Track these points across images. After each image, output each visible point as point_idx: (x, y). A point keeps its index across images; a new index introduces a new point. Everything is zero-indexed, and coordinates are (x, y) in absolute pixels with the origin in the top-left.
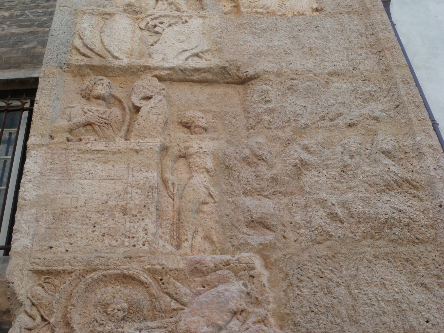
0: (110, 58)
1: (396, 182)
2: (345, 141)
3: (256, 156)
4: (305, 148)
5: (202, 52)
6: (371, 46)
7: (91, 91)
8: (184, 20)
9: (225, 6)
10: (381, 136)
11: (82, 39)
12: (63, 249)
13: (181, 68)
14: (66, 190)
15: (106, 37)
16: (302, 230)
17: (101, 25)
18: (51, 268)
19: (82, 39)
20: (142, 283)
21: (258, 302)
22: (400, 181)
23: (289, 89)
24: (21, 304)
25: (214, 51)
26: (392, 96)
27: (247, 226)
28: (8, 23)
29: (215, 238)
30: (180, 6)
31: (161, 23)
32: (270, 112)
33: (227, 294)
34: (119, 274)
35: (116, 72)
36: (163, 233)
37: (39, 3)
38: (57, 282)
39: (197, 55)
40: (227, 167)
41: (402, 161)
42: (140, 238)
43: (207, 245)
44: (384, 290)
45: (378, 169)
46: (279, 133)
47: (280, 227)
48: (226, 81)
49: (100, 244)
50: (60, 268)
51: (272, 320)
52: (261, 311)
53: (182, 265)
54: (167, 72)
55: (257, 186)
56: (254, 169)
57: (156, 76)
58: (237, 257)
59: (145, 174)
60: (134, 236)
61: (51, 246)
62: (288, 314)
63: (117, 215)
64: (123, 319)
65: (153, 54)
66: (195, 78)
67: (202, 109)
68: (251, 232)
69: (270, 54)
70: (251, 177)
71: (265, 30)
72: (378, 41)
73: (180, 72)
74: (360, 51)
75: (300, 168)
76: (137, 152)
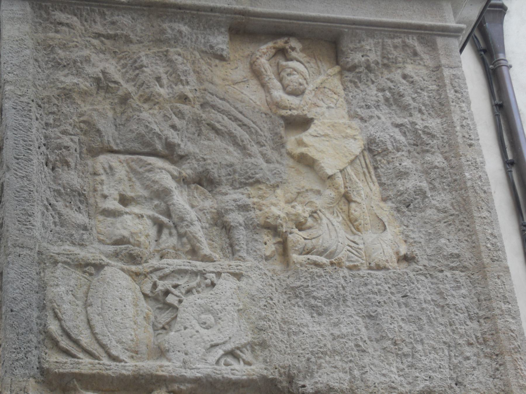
0: (105, 361)
5: (238, 348)
6: (485, 341)
8: (208, 281)
9: (266, 244)
11: (60, 320)
15: (96, 316)
17: (85, 288)
19: (60, 320)
25: (256, 345)
30: (198, 244)
31: (176, 286)
39: (232, 353)
54: (189, 386)
65: (168, 351)
69: (335, 351)
71: (327, 302)
74: (469, 352)
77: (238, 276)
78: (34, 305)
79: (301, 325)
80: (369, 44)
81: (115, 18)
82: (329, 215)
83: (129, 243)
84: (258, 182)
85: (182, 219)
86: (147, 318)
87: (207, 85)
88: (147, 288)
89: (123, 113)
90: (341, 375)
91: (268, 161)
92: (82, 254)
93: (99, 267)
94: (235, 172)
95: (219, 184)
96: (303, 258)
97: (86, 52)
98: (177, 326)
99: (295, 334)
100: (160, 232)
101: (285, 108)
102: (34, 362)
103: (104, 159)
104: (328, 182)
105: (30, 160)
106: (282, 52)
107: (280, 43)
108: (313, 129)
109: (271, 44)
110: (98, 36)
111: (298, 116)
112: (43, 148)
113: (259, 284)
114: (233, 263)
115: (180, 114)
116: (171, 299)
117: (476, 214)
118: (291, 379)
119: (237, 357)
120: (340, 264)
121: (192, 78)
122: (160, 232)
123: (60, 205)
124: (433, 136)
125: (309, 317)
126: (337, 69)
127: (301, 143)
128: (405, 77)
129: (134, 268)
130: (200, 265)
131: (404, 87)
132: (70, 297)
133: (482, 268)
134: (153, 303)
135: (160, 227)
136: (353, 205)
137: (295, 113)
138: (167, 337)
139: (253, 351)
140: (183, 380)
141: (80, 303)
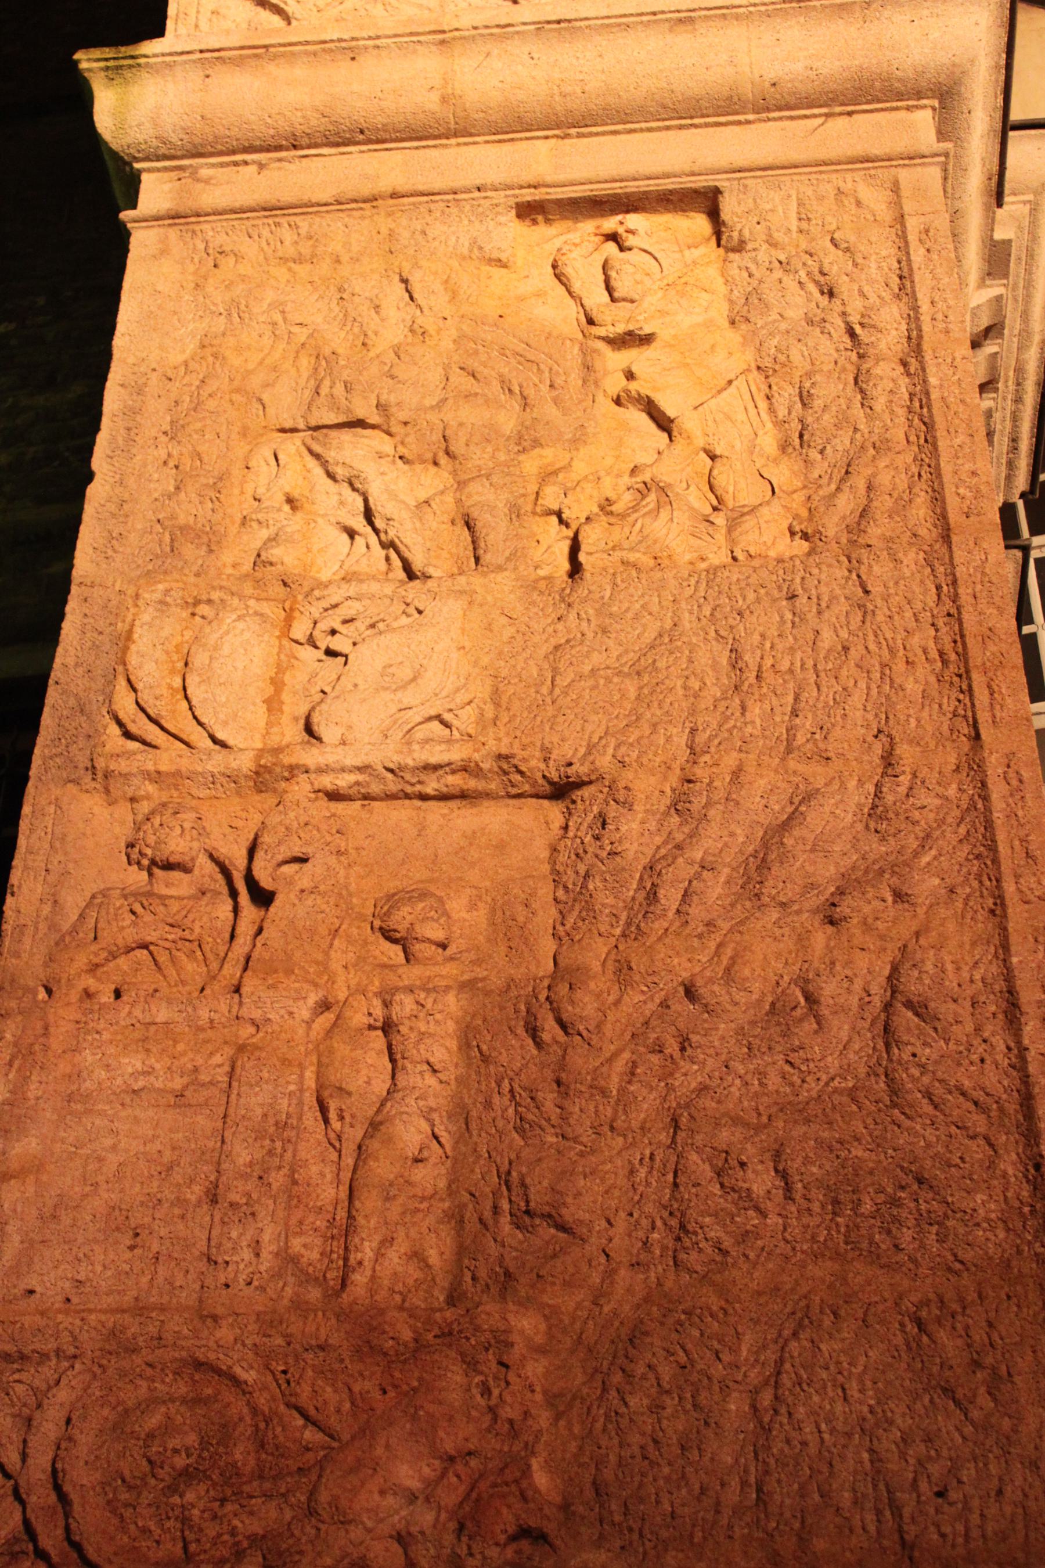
11: (135, 690)
13: (391, 766)
22: (938, 1090)
34: (181, 1360)
35: (218, 786)
36: (305, 1246)
42: (242, 1266)
44: (839, 1407)
48: (514, 791)
54: (352, 778)
60: (227, 1259)
61: (29, 1287)
73: (389, 775)
75: (672, 1057)
107: (610, 224)
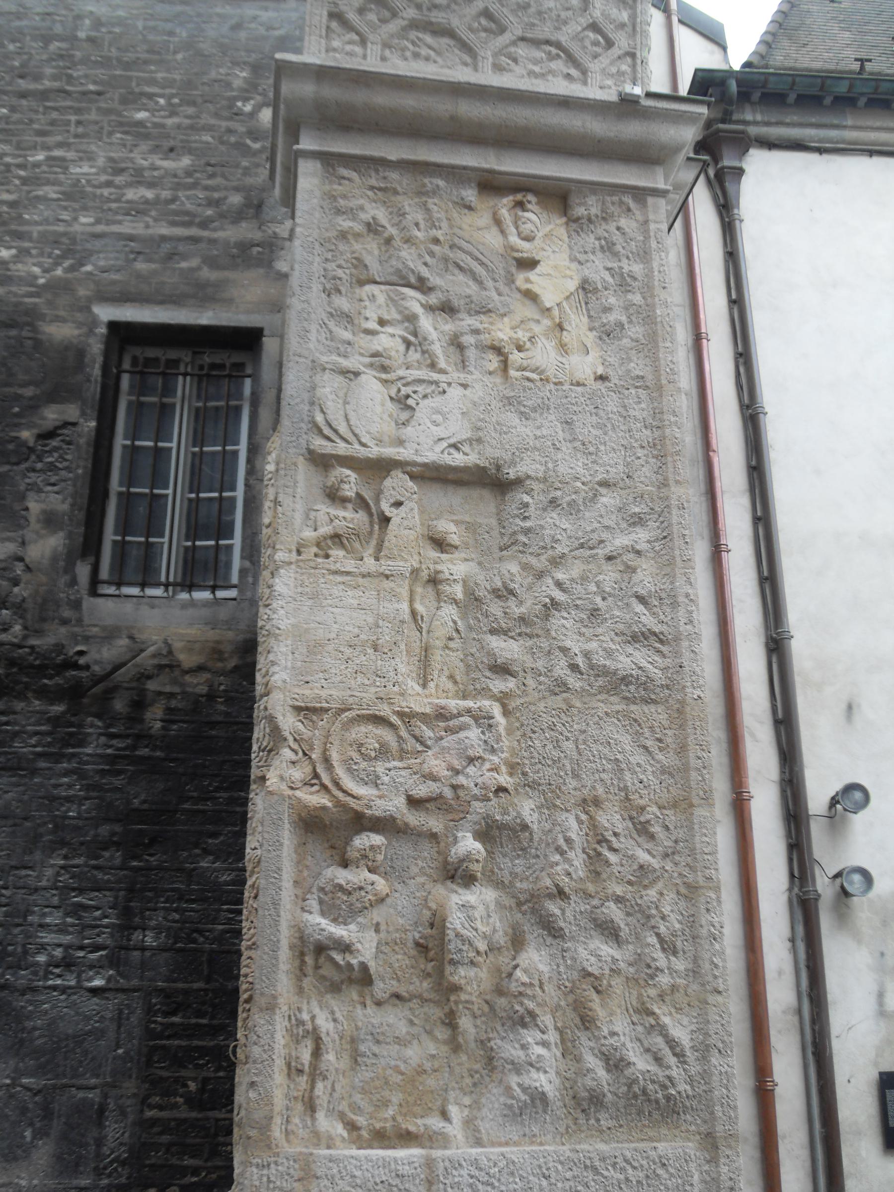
0: (357, 446)
1: (643, 634)
2: (601, 577)
3: (506, 588)
4: (559, 584)
6: (655, 445)
7: (337, 490)
10: (639, 575)
11: (324, 413)
12: (319, 685)
14: (318, 619)
16: (542, 678)
17: (345, 390)
18: (309, 705)
19: (324, 413)
20: (391, 725)
21: (493, 751)
23: (551, 502)
24: (285, 739)
26: (662, 522)
27: (490, 670)
28: (153, 213)
29: (458, 678)
31: (415, 392)
32: (527, 531)
33: (466, 741)
37: (198, 179)
38: (314, 718)
39: (455, 446)
40: (476, 599)
41: (655, 609)
43: (450, 685)
45: (628, 616)
46: (533, 561)
47: (521, 674)
49: (353, 682)
50: (318, 705)
51: (504, 769)
52: (496, 759)
53: (428, 710)
55: (504, 625)
56: (502, 604)
57: (408, 473)
58: (479, 704)
59: (396, 606)
62: (518, 764)
63: (369, 651)
64: (375, 758)
66: (450, 477)
67: (455, 518)
68: (493, 677)
70: (500, 614)
71: (534, 410)
72: (663, 438)
74: (640, 453)
76: (387, 577)
77: (465, 386)
78: (306, 401)
79: (512, 427)
80: (591, 200)
81: (387, 174)
82: (543, 339)
83: (382, 356)
84: (490, 311)
85: (425, 339)
86: (390, 416)
87: (456, 230)
88: (393, 394)
89: (386, 251)
90: (538, 466)
91: (500, 294)
92: (345, 363)
93: (357, 374)
94: (472, 302)
95: (458, 311)
96: (519, 374)
97: (361, 201)
98: (413, 423)
99: (505, 433)
100: (408, 348)
101: (518, 251)
102: (303, 443)
103: (369, 288)
104: (547, 313)
105: (310, 288)
106: (520, 205)
107: (519, 197)
108: (539, 269)
109: (511, 198)
110: (372, 188)
111: (528, 258)
112: (322, 279)
113: (481, 394)
114: (462, 376)
115: (432, 254)
116: (410, 402)
117: (661, 344)
118: (498, 468)
119: (458, 449)
120: (547, 380)
121: (444, 224)
122: (408, 348)
123: (331, 324)
124: (635, 279)
125: (518, 421)
126: (564, 220)
127: (528, 280)
128: (618, 228)
129: (384, 376)
130: (435, 376)
131: (617, 237)
132: (334, 397)
133: (660, 388)
134: (397, 404)
135: (408, 344)
136: (565, 333)
137: (525, 255)
138: (404, 431)
139: (471, 445)
140: (414, 464)
141: (341, 401)
